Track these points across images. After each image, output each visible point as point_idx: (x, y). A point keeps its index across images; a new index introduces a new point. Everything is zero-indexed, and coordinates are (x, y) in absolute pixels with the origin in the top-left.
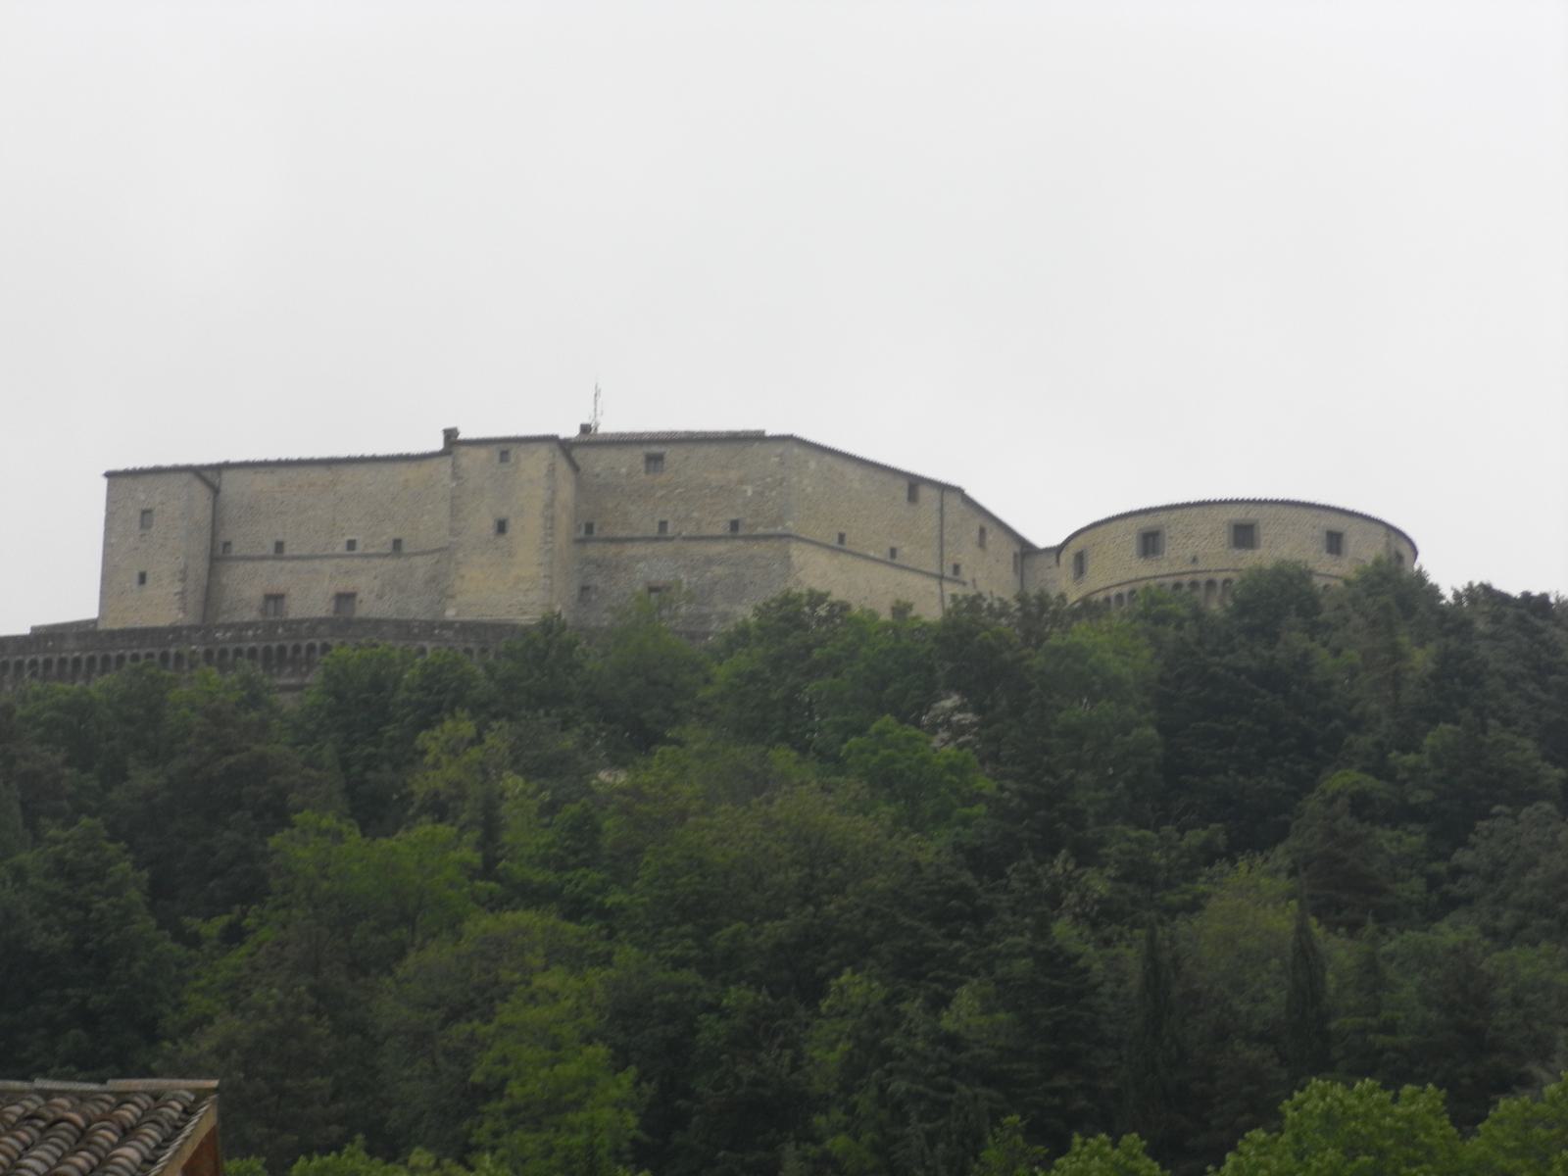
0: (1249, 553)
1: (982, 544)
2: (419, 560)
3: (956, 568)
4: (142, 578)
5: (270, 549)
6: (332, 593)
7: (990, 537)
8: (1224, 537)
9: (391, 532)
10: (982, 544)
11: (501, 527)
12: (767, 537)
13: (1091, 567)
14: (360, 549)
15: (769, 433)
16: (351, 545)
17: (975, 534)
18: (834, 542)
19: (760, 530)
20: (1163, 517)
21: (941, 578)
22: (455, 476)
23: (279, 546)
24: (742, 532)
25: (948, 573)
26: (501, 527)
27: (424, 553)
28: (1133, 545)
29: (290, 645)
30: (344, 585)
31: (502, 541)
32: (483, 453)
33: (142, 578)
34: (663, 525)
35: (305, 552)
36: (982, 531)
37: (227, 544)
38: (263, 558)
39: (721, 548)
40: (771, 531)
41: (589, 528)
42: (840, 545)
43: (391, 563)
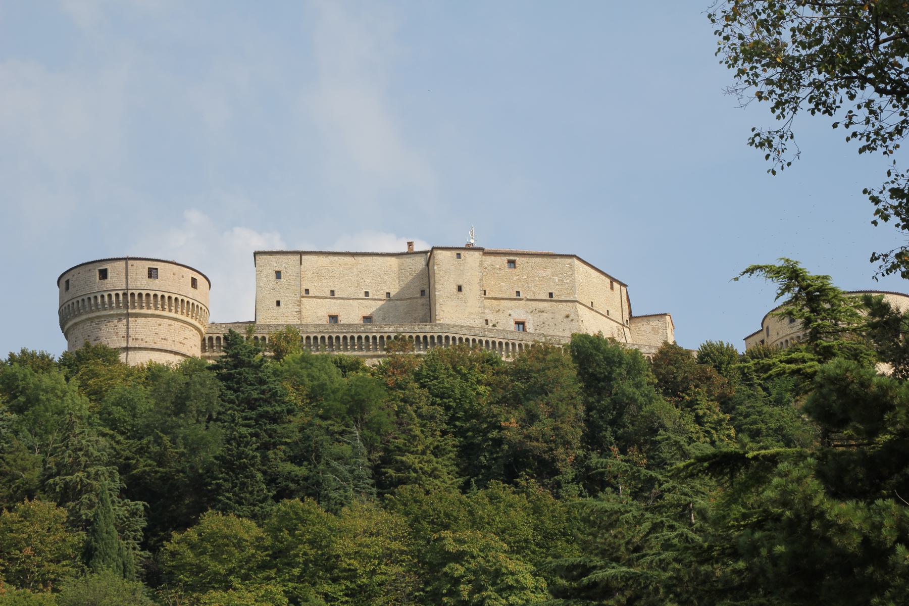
4: (278, 303)
5: (328, 294)
11: (460, 289)
14: (370, 294)
16: (367, 294)
19: (563, 298)
23: (332, 292)
24: (554, 298)
26: (460, 289)
27: (401, 300)
31: (460, 295)
32: (448, 253)
33: (278, 303)
34: (518, 293)
37: (307, 291)
38: (326, 298)
39: (546, 304)
40: (568, 299)
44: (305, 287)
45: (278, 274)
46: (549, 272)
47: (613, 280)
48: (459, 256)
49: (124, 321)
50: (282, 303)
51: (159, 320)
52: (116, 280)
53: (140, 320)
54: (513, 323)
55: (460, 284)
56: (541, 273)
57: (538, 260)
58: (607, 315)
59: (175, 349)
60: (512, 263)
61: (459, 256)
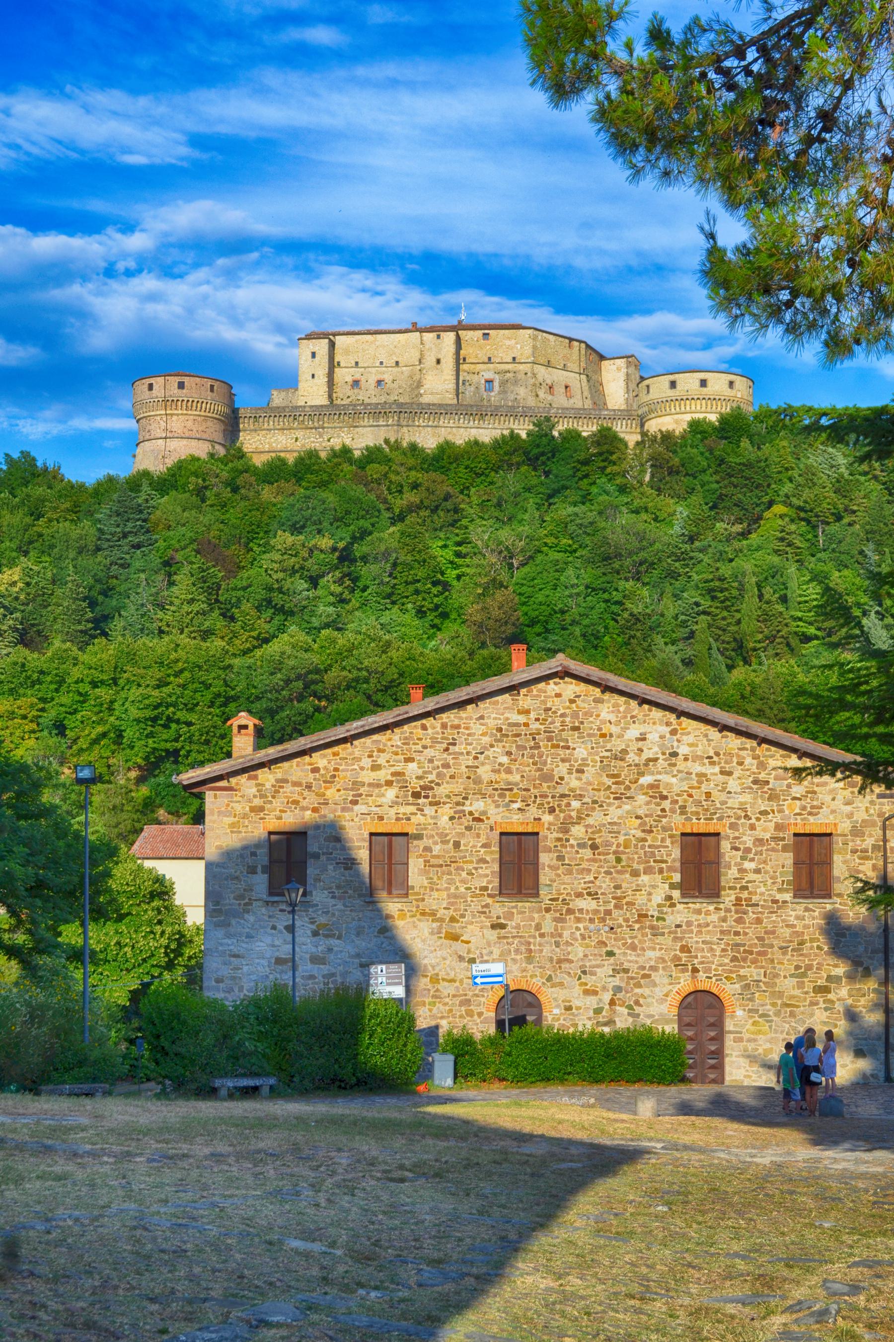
0: (704, 389)
4: (313, 376)
8: (698, 383)
9: (396, 359)
11: (438, 361)
15: (524, 324)
16: (381, 363)
23: (357, 363)
26: (438, 361)
28: (667, 385)
30: (380, 377)
33: (313, 376)
34: (490, 359)
37: (339, 363)
42: (548, 365)
43: (396, 369)
45: (314, 355)
46: (513, 342)
47: (571, 340)
48: (438, 337)
51: (187, 417)
53: (175, 418)
54: (483, 382)
56: (508, 342)
57: (506, 332)
58: (565, 368)
59: (198, 436)
60: (486, 335)
61: (438, 337)
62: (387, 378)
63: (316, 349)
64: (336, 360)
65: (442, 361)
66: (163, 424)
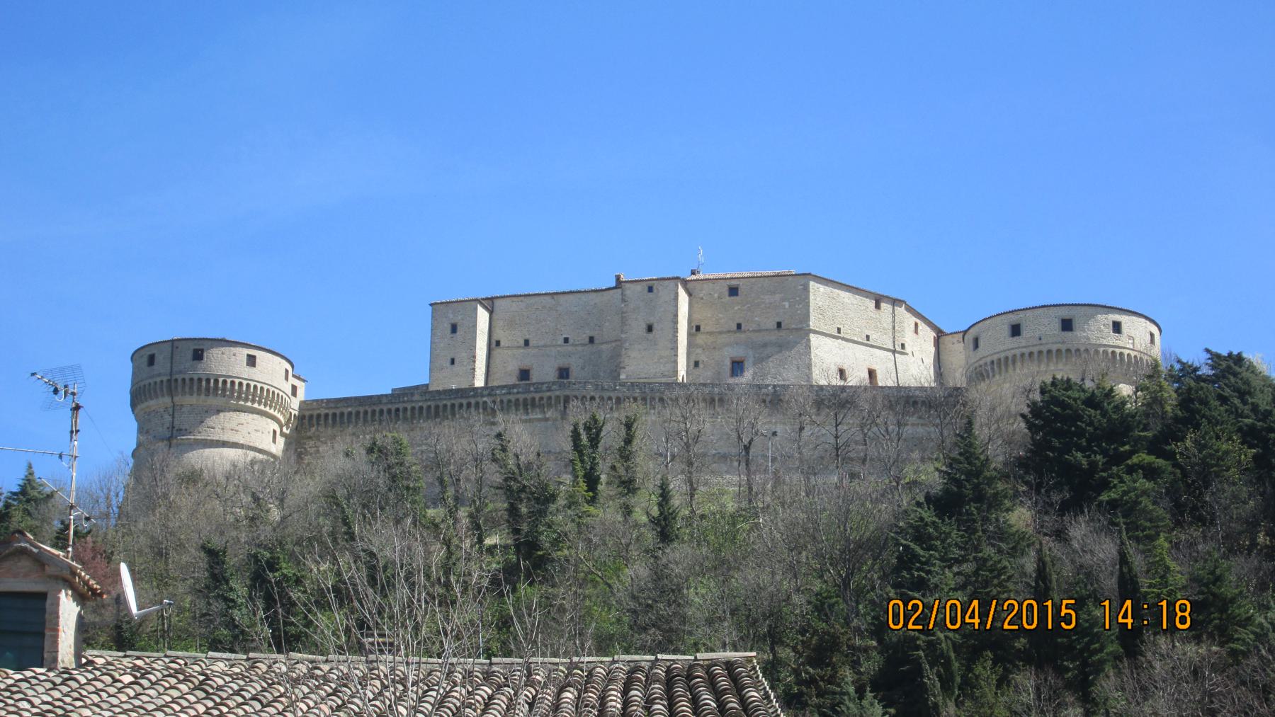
1: (916, 332)
2: (604, 347)
3: (903, 345)
4: (453, 362)
5: (522, 343)
6: (556, 366)
7: (920, 328)
8: (1057, 325)
9: (589, 333)
10: (916, 332)
11: (650, 329)
12: (797, 329)
13: (981, 343)
14: (571, 341)
16: (566, 340)
17: (913, 326)
18: (835, 332)
20: (1022, 315)
21: (894, 352)
22: (623, 301)
25: (898, 349)
26: (650, 329)
28: (1006, 330)
29: (537, 396)
30: (563, 362)
31: (651, 336)
32: (638, 287)
33: (453, 362)
34: (739, 326)
35: (542, 343)
36: (916, 325)
37: (498, 343)
41: (698, 328)
42: (838, 335)
44: (495, 338)
45: (454, 329)
46: (778, 297)
48: (650, 289)
49: (171, 410)
50: (457, 361)
52: (162, 365)
55: (652, 320)
58: (867, 342)
61: (650, 289)
62: (575, 364)
63: (458, 319)
64: (495, 338)
65: (655, 326)
66: (168, 418)
